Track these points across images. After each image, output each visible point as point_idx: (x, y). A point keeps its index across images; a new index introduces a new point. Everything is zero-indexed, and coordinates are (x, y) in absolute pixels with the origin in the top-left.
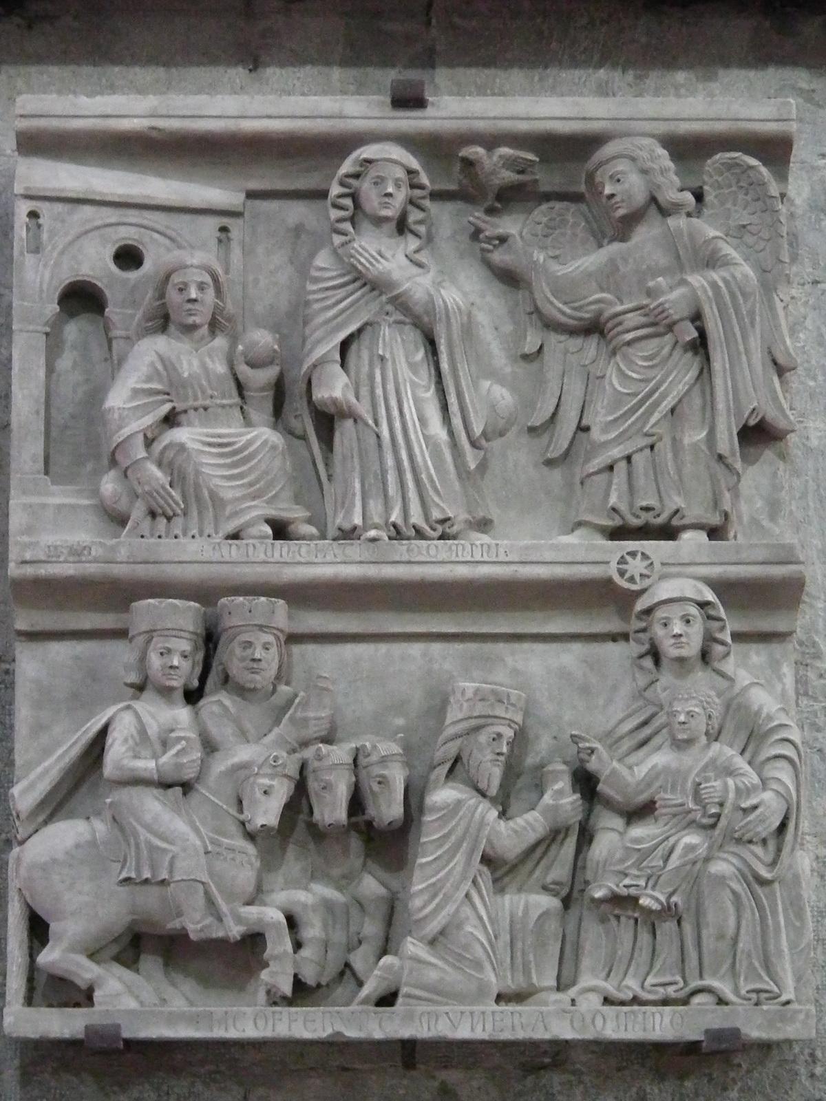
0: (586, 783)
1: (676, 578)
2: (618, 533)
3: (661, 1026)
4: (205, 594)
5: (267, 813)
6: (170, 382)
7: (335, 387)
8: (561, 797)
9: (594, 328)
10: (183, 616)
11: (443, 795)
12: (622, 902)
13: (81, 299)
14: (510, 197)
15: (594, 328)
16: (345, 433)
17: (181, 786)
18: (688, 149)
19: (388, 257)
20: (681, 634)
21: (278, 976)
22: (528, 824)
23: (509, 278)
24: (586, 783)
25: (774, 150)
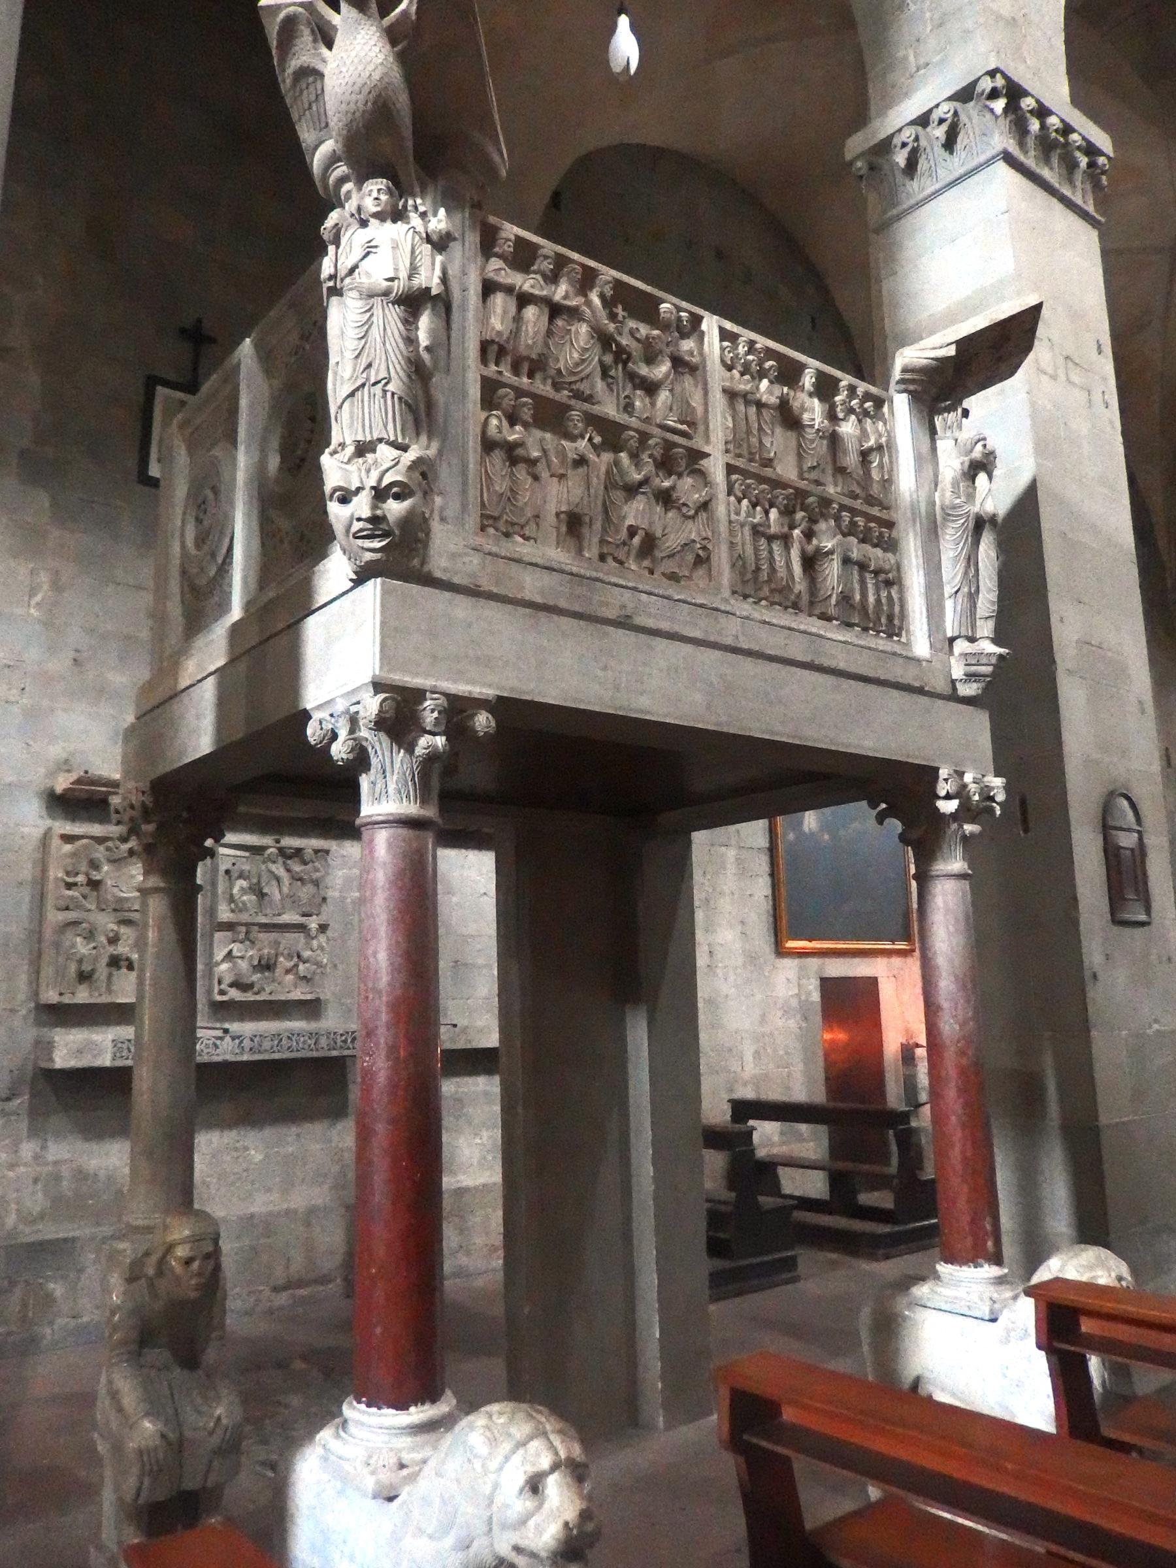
0: (299, 956)
1: (313, 926)
2: (303, 916)
3: (309, 997)
4: (246, 925)
5: (256, 963)
6: (242, 889)
7: (265, 891)
8: (295, 959)
9: (300, 879)
10: (243, 929)
11: (281, 959)
12: (305, 977)
13: (227, 872)
14: (290, 858)
15: (300, 879)
16: (266, 898)
17: (242, 958)
18: (316, 851)
19: (273, 867)
20: (313, 933)
21: (256, 989)
22: (292, 963)
23: (288, 870)
24: (299, 956)
25: (327, 852)
